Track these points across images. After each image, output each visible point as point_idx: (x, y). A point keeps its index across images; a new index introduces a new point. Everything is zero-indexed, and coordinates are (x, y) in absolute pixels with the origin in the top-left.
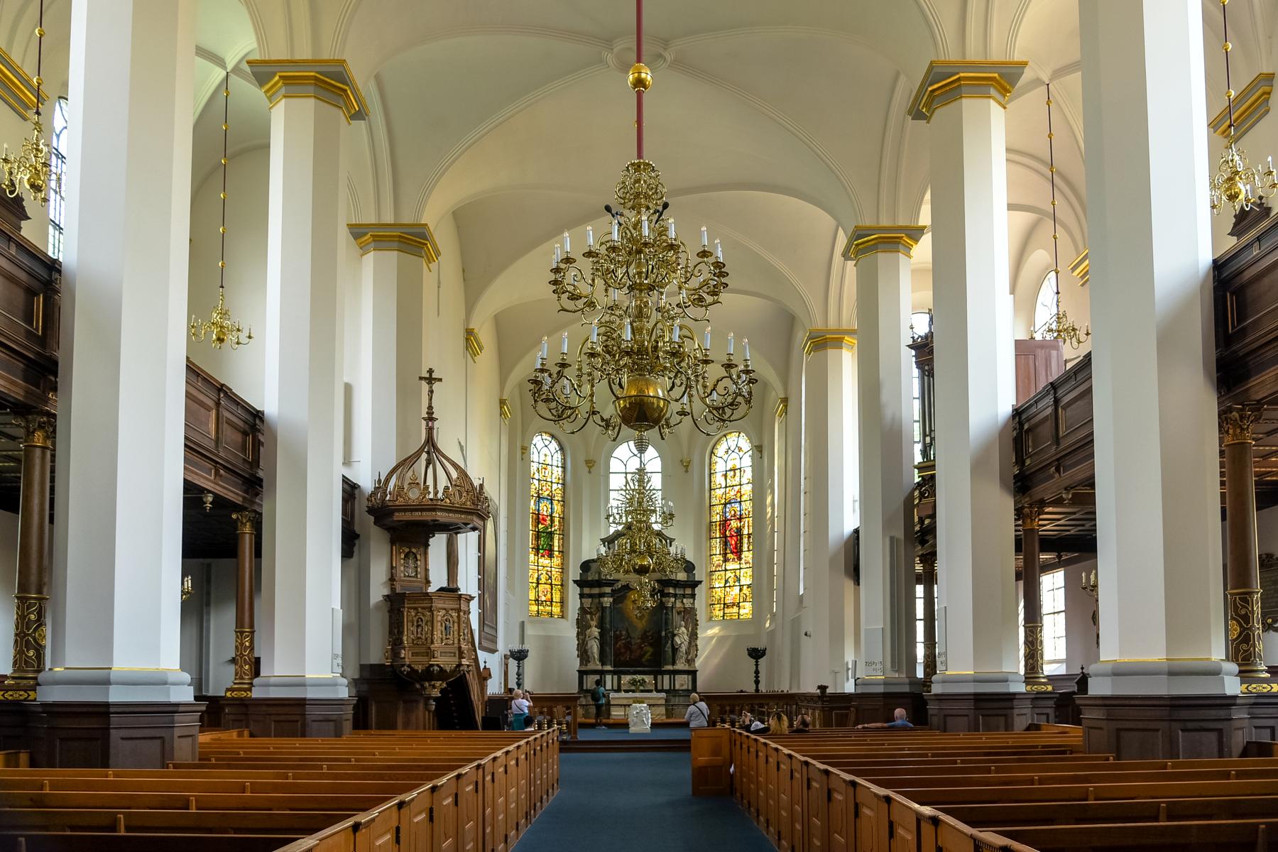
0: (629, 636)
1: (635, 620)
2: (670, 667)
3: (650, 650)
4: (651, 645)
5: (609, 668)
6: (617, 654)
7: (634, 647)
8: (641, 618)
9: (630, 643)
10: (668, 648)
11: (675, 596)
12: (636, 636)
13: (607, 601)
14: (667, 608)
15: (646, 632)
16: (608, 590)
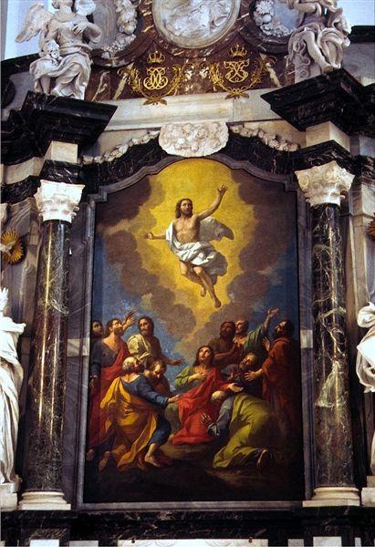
0: (157, 353)
1: (181, 282)
2: (334, 496)
3: (251, 413)
4: (253, 390)
5: (50, 501)
6: (103, 438)
7: (176, 403)
8: (207, 275)
9: (159, 383)
10: (330, 395)
11: (355, 164)
12: (187, 347)
13: (59, 200)
14: (318, 212)
15: (229, 333)
16: (64, 152)
